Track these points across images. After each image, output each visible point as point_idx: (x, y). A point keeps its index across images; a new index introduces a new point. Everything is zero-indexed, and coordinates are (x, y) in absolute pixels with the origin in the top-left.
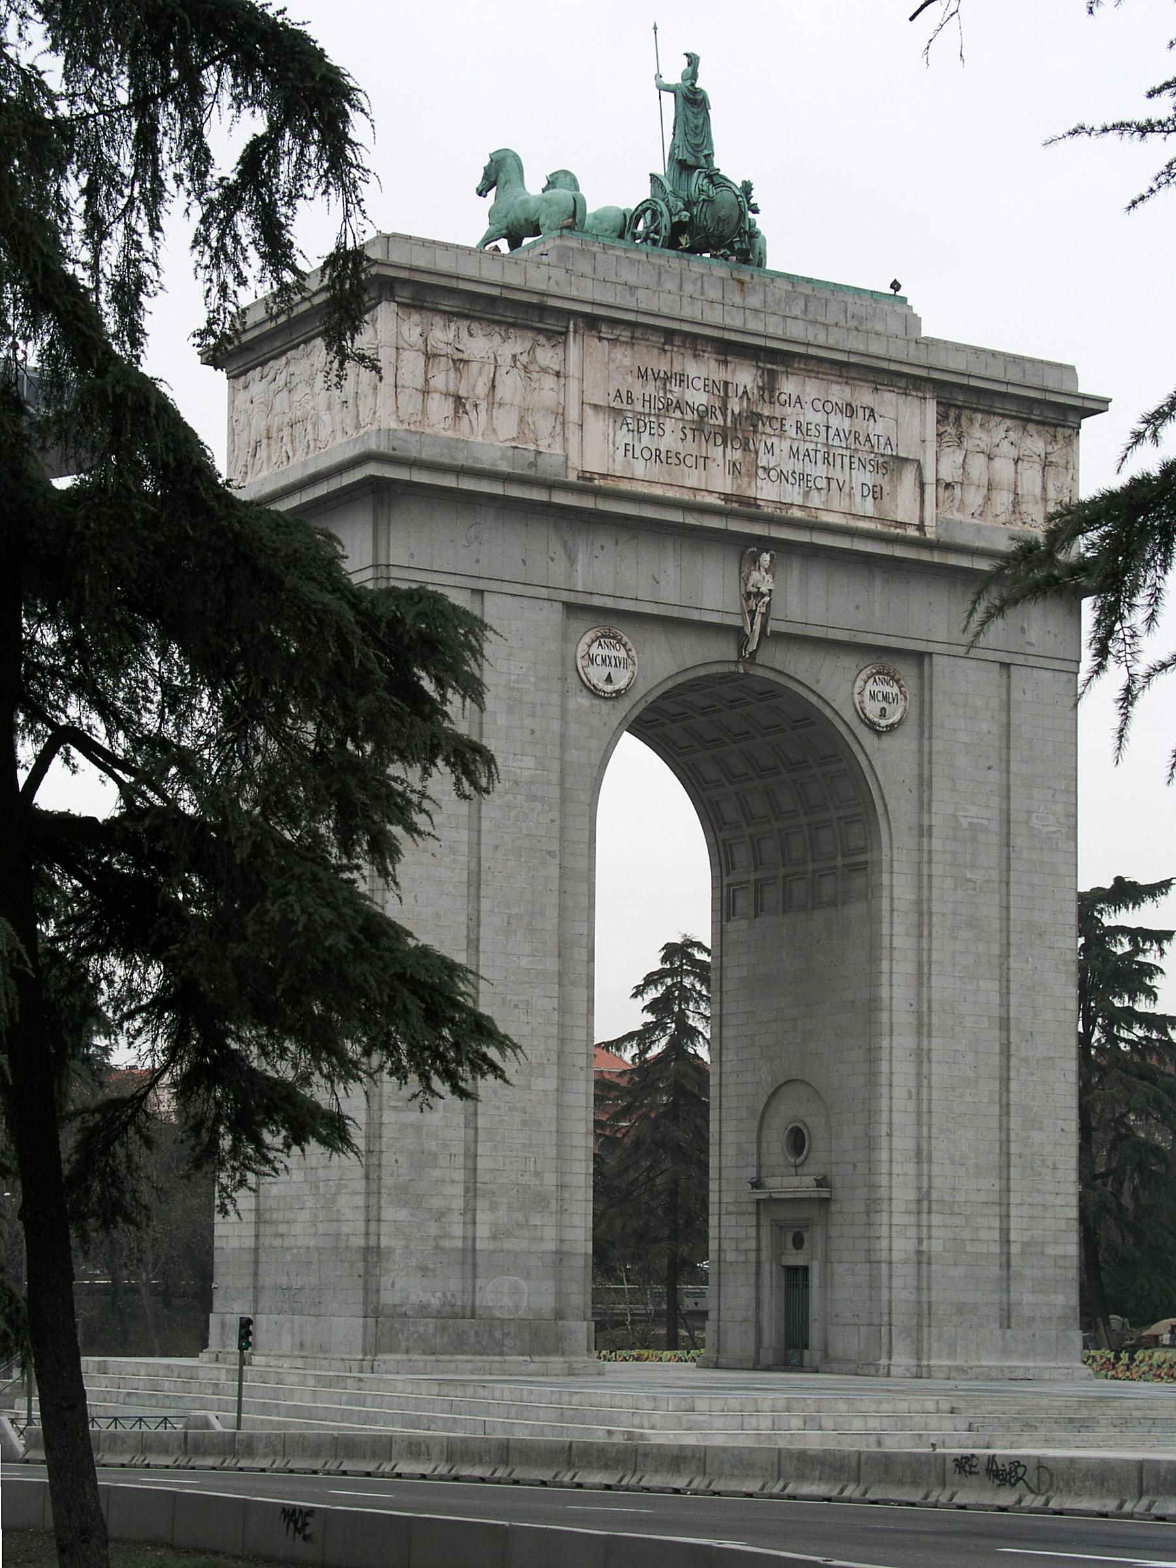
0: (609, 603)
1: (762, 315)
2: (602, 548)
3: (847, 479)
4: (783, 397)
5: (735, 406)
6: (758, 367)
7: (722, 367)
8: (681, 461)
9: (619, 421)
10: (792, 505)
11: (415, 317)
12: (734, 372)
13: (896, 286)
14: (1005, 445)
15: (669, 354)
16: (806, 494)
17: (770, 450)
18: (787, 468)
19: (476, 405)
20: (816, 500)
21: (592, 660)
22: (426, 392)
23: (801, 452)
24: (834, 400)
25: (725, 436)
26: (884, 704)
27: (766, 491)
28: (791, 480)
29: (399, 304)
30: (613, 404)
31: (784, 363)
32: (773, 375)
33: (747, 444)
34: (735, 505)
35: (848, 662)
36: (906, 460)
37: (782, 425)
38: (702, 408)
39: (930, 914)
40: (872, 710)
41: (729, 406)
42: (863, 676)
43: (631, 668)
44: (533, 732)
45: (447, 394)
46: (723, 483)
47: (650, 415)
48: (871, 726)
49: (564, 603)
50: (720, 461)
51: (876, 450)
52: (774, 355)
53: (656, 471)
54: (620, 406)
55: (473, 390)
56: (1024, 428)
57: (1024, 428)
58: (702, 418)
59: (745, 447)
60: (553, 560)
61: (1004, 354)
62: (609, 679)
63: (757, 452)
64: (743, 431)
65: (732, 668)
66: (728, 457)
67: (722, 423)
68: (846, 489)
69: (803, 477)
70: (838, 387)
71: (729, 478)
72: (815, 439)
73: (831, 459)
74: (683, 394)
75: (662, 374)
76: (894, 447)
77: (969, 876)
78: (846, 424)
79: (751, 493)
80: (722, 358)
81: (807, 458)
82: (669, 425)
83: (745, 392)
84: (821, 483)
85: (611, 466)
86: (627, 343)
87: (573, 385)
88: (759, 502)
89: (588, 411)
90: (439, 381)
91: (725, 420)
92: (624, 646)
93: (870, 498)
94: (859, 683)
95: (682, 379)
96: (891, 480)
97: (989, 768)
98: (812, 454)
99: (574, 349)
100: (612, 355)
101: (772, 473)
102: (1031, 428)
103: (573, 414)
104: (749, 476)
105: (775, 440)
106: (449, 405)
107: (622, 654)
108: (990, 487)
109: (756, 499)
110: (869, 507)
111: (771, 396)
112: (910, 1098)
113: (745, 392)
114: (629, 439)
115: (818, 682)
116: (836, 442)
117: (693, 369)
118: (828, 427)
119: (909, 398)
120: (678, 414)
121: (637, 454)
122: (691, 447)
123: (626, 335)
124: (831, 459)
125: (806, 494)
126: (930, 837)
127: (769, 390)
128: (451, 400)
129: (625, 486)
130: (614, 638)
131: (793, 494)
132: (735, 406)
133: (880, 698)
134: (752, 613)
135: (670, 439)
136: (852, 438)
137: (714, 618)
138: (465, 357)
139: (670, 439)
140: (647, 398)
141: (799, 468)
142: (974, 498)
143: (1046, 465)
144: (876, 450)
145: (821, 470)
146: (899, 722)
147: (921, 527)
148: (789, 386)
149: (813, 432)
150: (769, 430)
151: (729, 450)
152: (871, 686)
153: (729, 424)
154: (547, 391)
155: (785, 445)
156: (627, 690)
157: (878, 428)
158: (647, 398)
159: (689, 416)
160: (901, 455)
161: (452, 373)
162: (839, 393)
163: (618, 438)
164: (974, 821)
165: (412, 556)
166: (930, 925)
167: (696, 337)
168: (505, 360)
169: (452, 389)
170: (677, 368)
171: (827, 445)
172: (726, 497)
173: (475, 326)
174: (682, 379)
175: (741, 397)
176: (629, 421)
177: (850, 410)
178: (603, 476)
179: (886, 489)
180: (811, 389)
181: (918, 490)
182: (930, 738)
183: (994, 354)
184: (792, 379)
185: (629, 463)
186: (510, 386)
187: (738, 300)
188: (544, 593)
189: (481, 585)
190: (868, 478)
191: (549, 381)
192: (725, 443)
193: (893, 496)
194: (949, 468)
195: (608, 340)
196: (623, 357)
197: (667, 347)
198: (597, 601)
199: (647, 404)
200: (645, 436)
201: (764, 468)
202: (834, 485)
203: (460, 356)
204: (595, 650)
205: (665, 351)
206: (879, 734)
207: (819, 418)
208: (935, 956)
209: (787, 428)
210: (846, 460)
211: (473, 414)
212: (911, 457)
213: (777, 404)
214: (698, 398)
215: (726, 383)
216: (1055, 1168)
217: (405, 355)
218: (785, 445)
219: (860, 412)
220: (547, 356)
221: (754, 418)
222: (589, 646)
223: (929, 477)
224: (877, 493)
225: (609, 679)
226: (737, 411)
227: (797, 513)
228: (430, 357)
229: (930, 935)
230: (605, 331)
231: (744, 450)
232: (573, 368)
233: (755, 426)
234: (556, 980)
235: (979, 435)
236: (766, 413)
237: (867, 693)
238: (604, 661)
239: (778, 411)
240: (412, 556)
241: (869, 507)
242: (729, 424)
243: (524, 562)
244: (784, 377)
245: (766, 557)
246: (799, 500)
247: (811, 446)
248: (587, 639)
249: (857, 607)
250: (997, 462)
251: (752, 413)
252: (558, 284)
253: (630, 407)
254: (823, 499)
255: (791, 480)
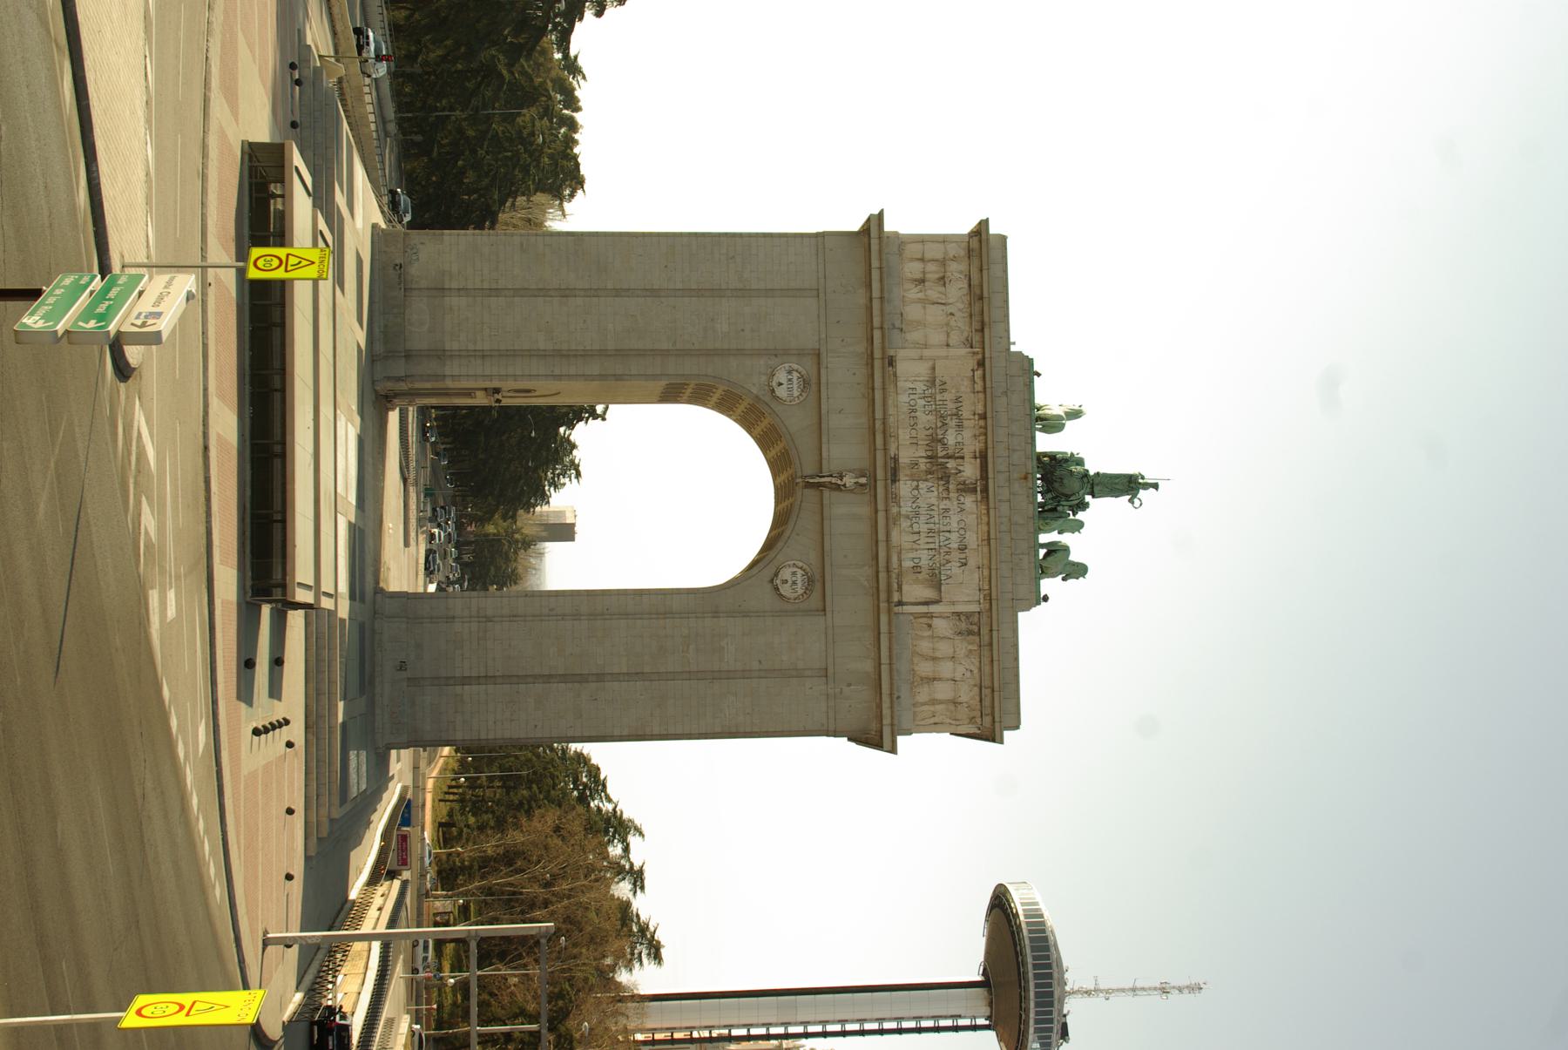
0: (823, 380)
1: (1007, 484)
2: (854, 374)
3: (922, 547)
4: (962, 499)
5: (951, 464)
6: (977, 480)
7: (972, 455)
8: (913, 426)
9: (928, 384)
10: (900, 507)
11: (963, 253)
12: (971, 463)
13: (1046, 599)
14: (961, 670)
15: (972, 417)
16: (907, 517)
17: (929, 490)
18: (921, 502)
19: (921, 291)
20: (905, 524)
21: (790, 372)
22: (922, 260)
23: (932, 513)
24: (967, 536)
25: (932, 458)
26: (790, 582)
27: (905, 487)
28: (914, 506)
29: (969, 242)
30: (937, 380)
31: (982, 498)
32: (974, 491)
33: (930, 473)
34: (893, 465)
35: (813, 557)
36: (940, 591)
37: (946, 498)
38: (945, 440)
39: (665, 618)
40: (786, 574)
41: (949, 460)
42: (805, 567)
43: (788, 399)
44: (743, 330)
45: (924, 273)
46: (905, 457)
47: (936, 405)
48: (776, 575)
49: (819, 349)
50: (917, 455)
51: (942, 568)
52: (985, 490)
53: (905, 409)
54: (937, 385)
55: (931, 289)
56: (975, 685)
57: (975, 685)
58: (940, 441)
59: (929, 472)
60: (843, 341)
61: (1018, 667)
62: (780, 384)
63: (926, 480)
64: (937, 470)
65: (799, 474)
66: (919, 459)
67: (939, 455)
68: (915, 546)
69: (917, 514)
70: (975, 539)
71: (907, 461)
72: (941, 522)
73: (930, 535)
74: (951, 428)
75: (960, 413)
76: (947, 581)
77: (692, 647)
78: (956, 546)
79: (902, 476)
80: (978, 455)
81: (929, 517)
82: (931, 417)
83: (960, 471)
84: (916, 530)
85: (902, 379)
86: (974, 388)
87: (943, 352)
88: (897, 483)
89: (931, 363)
90: (931, 267)
91: (941, 457)
92: (801, 395)
93: (912, 564)
94: (800, 564)
95: (960, 426)
96: (927, 580)
97: (760, 662)
98: (932, 520)
99: (964, 351)
100: (965, 379)
101: (916, 492)
102: (976, 690)
103: (927, 353)
104: (912, 475)
105: (936, 493)
106: (918, 276)
107: (796, 393)
108: (934, 659)
109: (899, 480)
110: (907, 564)
111: (962, 490)
112: (550, 610)
113: (960, 471)
114: (919, 391)
115: (798, 535)
116: (942, 538)
117: (967, 434)
118: (949, 532)
119: (978, 592)
120: (939, 424)
121: (912, 397)
122: (922, 434)
123: (979, 387)
124: (930, 535)
125: (907, 517)
126: (714, 617)
127: (966, 489)
128: (921, 276)
129: (891, 389)
130: (804, 387)
131: (906, 508)
132: (951, 464)
133: (794, 579)
134: (831, 476)
135: (924, 419)
136: (948, 550)
137: (825, 454)
138: (947, 285)
139: (924, 419)
140: (945, 403)
141: (922, 511)
142: (925, 646)
143: (955, 703)
144: (942, 568)
145: (924, 528)
146: (781, 595)
147: (900, 603)
148: (969, 501)
149: (946, 522)
150: (941, 490)
151: (924, 460)
152: (800, 572)
153: (940, 460)
154: (937, 337)
155: (934, 501)
156: (776, 398)
157: (954, 568)
158: (945, 403)
159: (940, 432)
160: (943, 588)
161: (937, 276)
162: (972, 539)
163: (919, 383)
164: (726, 650)
165: (831, 250)
166: (658, 618)
167: (986, 434)
168: (949, 309)
169: (928, 276)
170: (966, 423)
171: (939, 532)
172: (896, 459)
173: (965, 291)
174: (960, 426)
175: (957, 469)
176: (930, 391)
177: (962, 549)
178: (895, 375)
179: (920, 576)
180: (971, 520)
181: (923, 600)
182: (773, 616)
183: (1016, 659)
184: (974, 506)
185: (906, 391)
186: (935, 314)
187: (1016, 475)
188: (823, 336)
189: (821, 295)
190: (924, 562)
191: (943, 338)
192: (928, 457)
193: (917, 581)
194: (941, 626)
195: (973, 376)
196: (965, 386)
197: (977, 417)
198: (823, 371)
199: (941, 403)
200: (922, 402)
201: (918, 486)
202: (916, 537)
203: (947, 282)
204: (795, 375)
205: (974, 414)
206: (772, 581)
207: (954, 526)
208: (639, 622)
209: (945, 502)
210: (932, 546)
211: (916, 290)
212: (942, 594)
213: (957, 495)
214: (951, 438)
215: (963, 458)
216: (512, 720)
217: (941, 246)
218: (934, 501)
219: (963, 556)
220: (955, 338)
221: (945, 477)
222: (797, 371)
223: (933, 608)
224: (916, 569)
225: (780, 384)
226: (948, 465)
227: (894, 510)
228: (943, 262)
229: (651, 619)
230: (979, 373)
231: (926, 472)
232: (952, 352)
233: (942, 478)
234: (602, 348)
235: (962, 646)
236: (951, 487)
237: (795, 569)
238: (790, 380)
239: (953, 495)
240: (831, 250)
241: (907, 564)
242: (940, 460)
243: (838, 322)
244: (974, 499)
245: (863, 480)
246: (903, 512)
247: (937, 521)
248: (800, 369)
249: (845, 556)
250: (950, 664)
251: (949, 477)
252: (999, 343)
253: (937, 391)
254: (907, 529)
255: (914, 506)
